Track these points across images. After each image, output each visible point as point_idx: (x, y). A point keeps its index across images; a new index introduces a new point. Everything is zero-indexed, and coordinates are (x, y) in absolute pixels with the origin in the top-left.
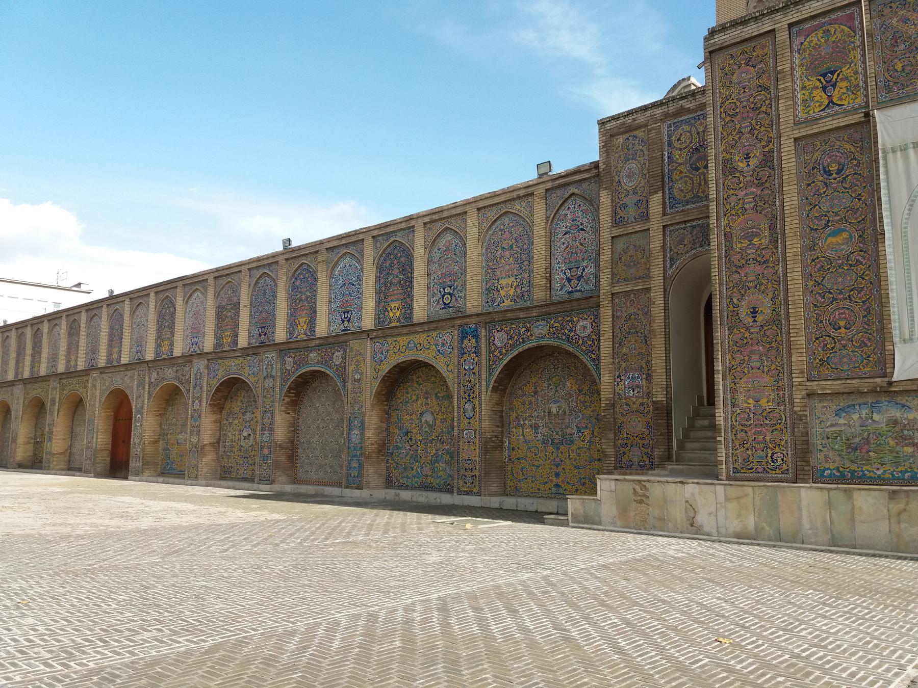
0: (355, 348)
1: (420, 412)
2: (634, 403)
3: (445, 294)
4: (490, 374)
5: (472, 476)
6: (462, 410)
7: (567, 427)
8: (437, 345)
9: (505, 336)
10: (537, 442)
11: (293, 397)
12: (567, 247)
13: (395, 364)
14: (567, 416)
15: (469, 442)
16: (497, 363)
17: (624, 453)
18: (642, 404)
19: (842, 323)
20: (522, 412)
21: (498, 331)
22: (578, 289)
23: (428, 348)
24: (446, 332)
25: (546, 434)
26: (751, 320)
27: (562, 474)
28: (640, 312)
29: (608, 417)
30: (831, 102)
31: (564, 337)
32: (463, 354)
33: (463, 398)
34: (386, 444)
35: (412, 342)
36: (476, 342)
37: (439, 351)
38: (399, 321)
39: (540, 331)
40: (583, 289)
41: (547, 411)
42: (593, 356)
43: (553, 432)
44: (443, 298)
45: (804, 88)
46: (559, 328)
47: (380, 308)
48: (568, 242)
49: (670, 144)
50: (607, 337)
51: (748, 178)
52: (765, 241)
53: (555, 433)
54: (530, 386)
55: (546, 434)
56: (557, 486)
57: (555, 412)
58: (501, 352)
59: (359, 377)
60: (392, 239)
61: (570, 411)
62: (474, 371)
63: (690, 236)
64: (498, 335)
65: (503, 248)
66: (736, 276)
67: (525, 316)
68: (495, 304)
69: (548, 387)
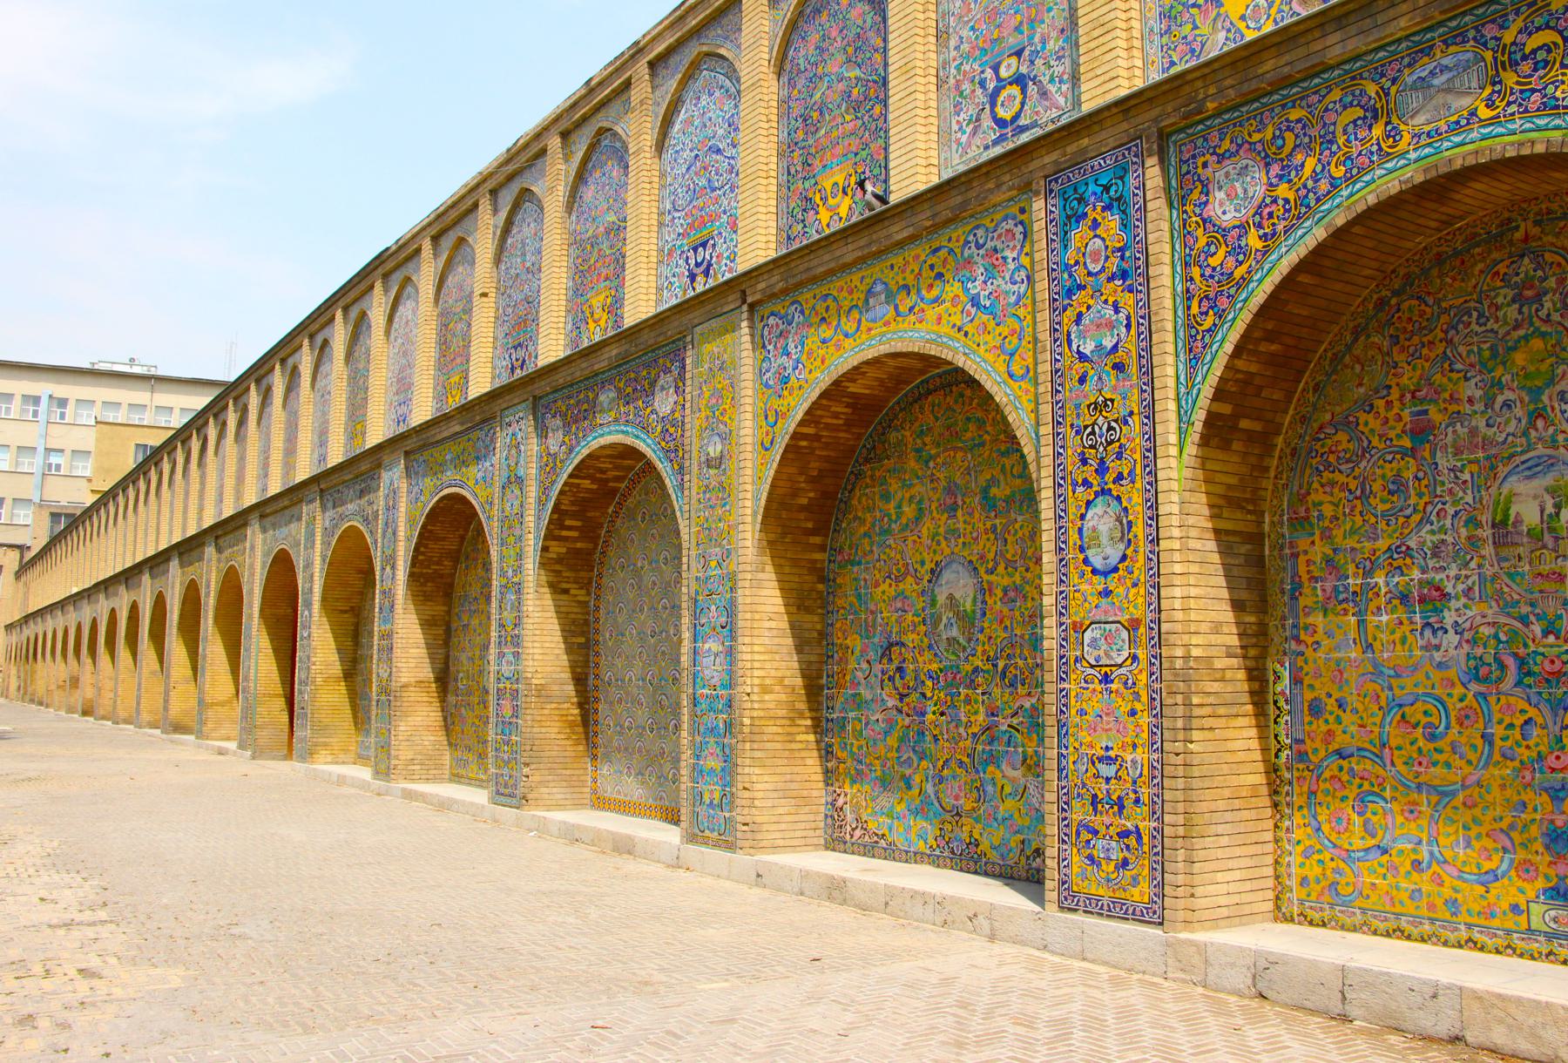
1: (928, 566)
4: (1192, 370)
5: (1124, 834)
6: (1073, 537)
10: (1436, 676)
11: (575, 540)
15: (1106, 679)
16: (1223, 303)
20: (1353, 532)
21: (1221, 158)
24: (998, 217)
25: (1486, 631)
32: (1070, 293)
33: (1075, 484)
34: (821, 688)
35: (879, 288)
41: (1485, 518)
43: (1524, 620)
44: (993, 105)
47: (793, 205)
53: (1537, 629)
54: (1389, 404)
55: (1486, 631)
58: (1239, 252)
59: (719, 448)
69: (1490, 403)
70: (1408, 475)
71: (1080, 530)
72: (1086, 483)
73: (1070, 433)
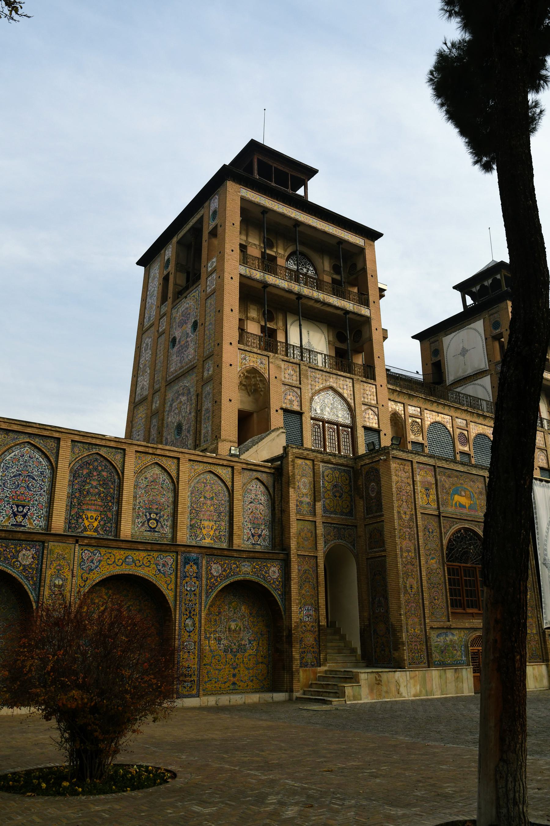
0: (57, 551)
2: (308, 626)
3: (151, 519)
5: (191, 681)
6: (183, 624)
7: (242, 640)
8: (157, 565)
9: (220, 568)
10: (220, 651)
12: (252, 512)
13: (108, 575)
14: (242, 632)
15: (189, 652)
16: (213, 588)
17: (304, 657)
18: (312, 626)
19: (436, 598)
20: (208, 627)
21: (214, 563)
22: (259, 543)
23: (148, 566)
24: (168, 555)
25: (227, 645)
26: (410, 591)
27: (237, 675)
28: (311, 570)
29: (296, 634)
30: (428, 502)
31: (262, 577)
32: (185, 577)
33: (184, 614)
35: (130, 557)
36: (198, 568)
37: (159, 570)
38: (96, 530)
39: (246, 569)
40: (261, 544)
42: (279, 592)
44: (148, 522)
45: (421, 492)
46: (259, 570)
47: (72, 514)
48: (252, 509)
49: (323, 477)
50: (295, 582)
51: (406, 524)
52: (413, 555)
56: (234, 684)
57: (233, 628)
58: (216, 580)
60: (94, 451)
61: (244, 628)
62: (195, 592)
63: (333, 532)
64: (214, 566)
65: (205, 497)
66: (404, 568)
67: (238, 556)
68: (197, 539)
69: (229, 610)
70: (217, 619)
71: (184, 623)
72: (186, 614)
73: (183, 604)
